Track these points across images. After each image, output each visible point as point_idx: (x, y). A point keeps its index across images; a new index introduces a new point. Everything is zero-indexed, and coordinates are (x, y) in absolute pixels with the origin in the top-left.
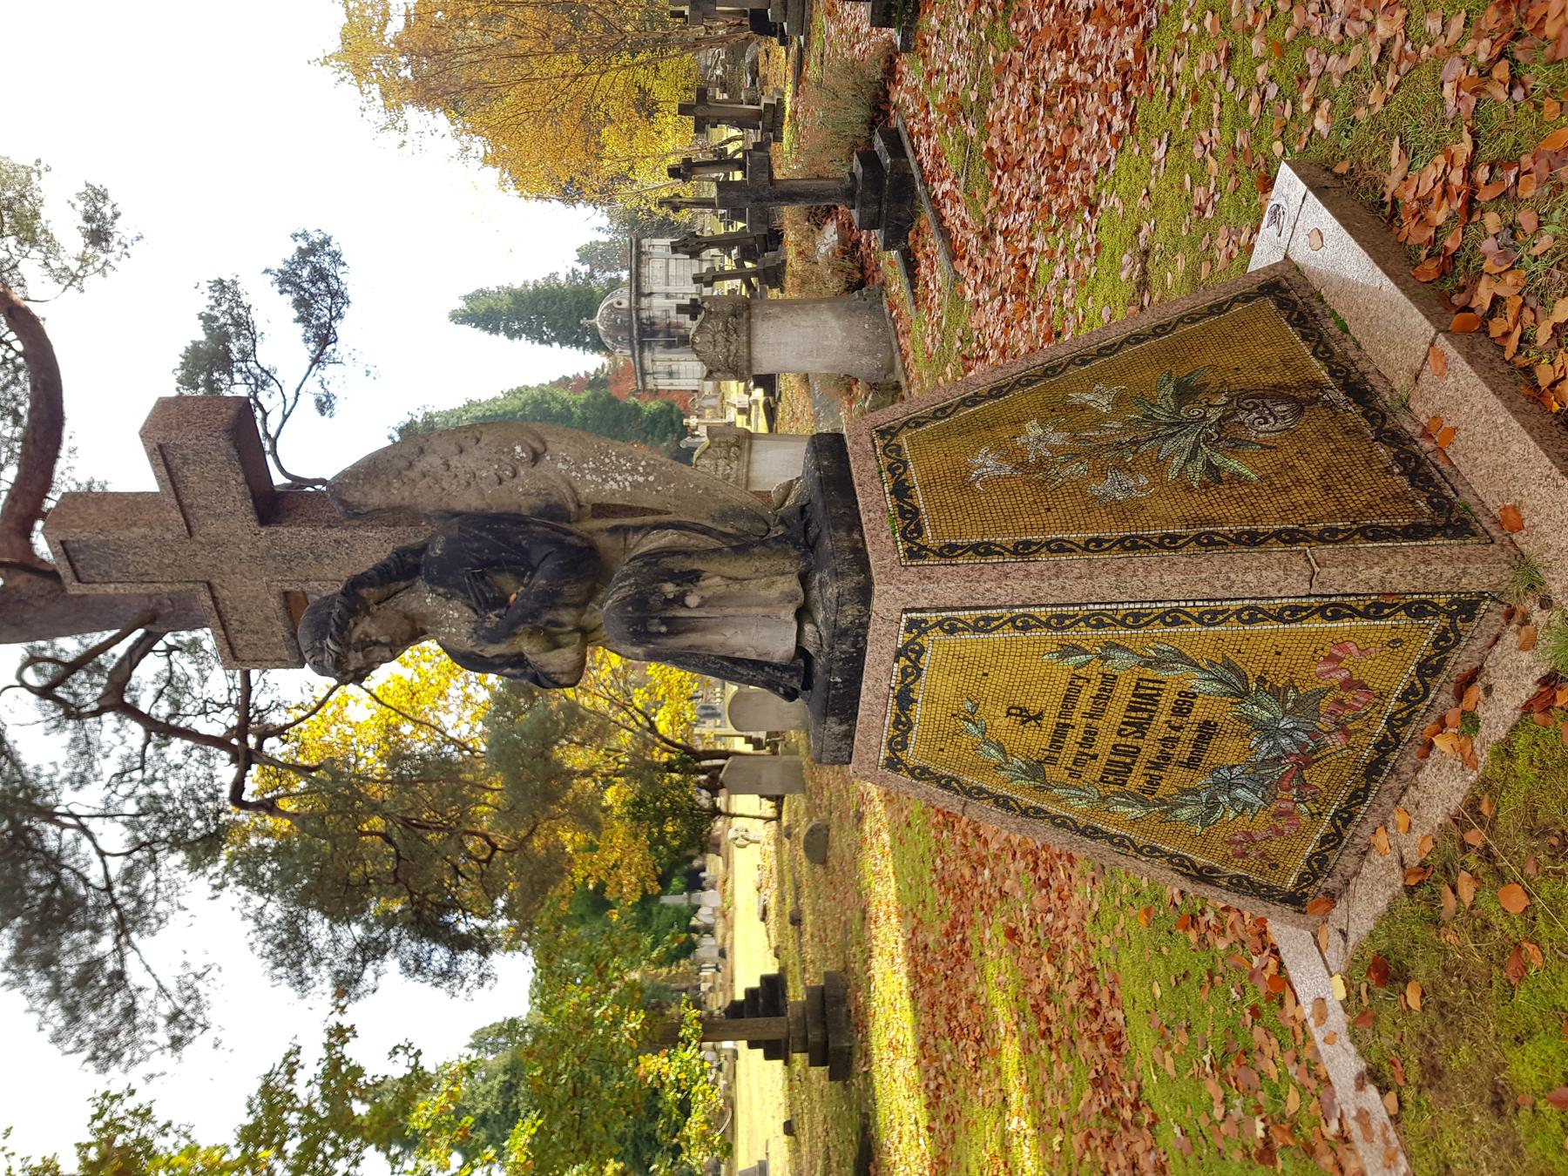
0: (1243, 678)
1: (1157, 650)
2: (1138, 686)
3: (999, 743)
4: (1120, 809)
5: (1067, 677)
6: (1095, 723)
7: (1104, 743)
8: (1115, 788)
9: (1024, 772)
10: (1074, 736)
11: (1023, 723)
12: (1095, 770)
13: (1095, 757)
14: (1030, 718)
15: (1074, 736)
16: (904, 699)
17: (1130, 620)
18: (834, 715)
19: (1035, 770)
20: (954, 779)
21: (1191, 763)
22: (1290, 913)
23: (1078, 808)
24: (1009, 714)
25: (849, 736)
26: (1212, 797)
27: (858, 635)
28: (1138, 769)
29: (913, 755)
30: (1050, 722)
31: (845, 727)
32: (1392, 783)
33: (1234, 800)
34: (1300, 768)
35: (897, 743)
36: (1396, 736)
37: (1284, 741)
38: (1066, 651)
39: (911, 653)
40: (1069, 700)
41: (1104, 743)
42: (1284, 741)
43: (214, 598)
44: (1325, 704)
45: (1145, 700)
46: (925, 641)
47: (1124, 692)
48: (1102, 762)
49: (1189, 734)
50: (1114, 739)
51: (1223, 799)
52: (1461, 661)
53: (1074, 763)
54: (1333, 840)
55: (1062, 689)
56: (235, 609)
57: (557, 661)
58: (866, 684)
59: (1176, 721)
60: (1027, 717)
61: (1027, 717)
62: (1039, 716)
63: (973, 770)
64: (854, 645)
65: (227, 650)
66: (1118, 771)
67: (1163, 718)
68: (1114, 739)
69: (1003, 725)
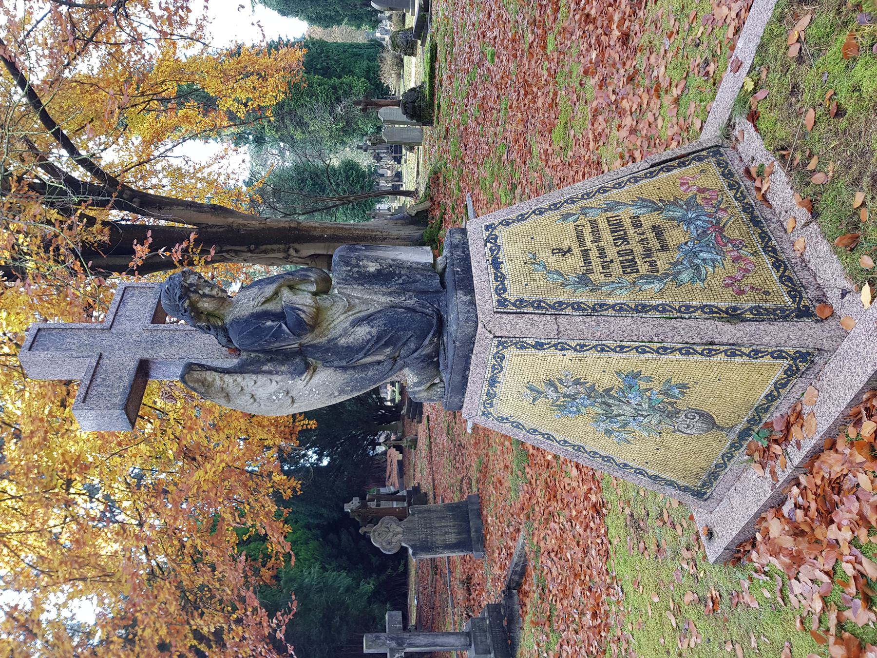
0: (653, 203)
1: (606, 204)
2: (608, 221)
3: (557, 271)
4: (647, 287)
5: (572, 228)
6: (600, 244)
7: (612, 252)
8: (634, 275)
9: (580, 283)
10: (594, 254)
11: (563, 256)
12: (616, 269)
13: (612, 261)
14: (566, 252)
15: (594, 254)
16: (496, 264)
17: (585, 197)
18: (461, 289)
19: (584, 280)
20: (541, 301)
21: (664, 248)
22: (813, 325)
23: (623, 297)
24: (554, 254)
25: (473, 303)
26: (690, 263)
27: (464, 248)
28: (639, 261)
29: (513, 293)
30: (577, 251)
31: (468, 297)
32: (772, 226)
33: (704, 260)
34: (720, 233)
35: (500, 290)
36: (747, 204)
37: (699, 223)
38: (565, 217)
39: (492, 240)
40: (580, 237)
41: (612, 252)
42: (699, 223)
43: (98, 363)
44: (699, 201)
45: (616, 226)
46: (496, 232)
47: (603, 225)
48: (617, 261)
49: (650, 235)
50: (615, 249)
51: (698, 261)
52: (737, 168)
53: (603, 268)
54: (778, 264)
55: (574, 233)
56: (106, 371)
57: (301, 302)
58: (474, 265)
59: (639, 231)
60: (565, 252)
61: (565, 252)
62: (570, 250)
63: (550, 292)
64: (463, 252)
65: (92, 371)
66: (629, 265)
67: (632, 232)
68: (615, 249)
69: (553, 261)
